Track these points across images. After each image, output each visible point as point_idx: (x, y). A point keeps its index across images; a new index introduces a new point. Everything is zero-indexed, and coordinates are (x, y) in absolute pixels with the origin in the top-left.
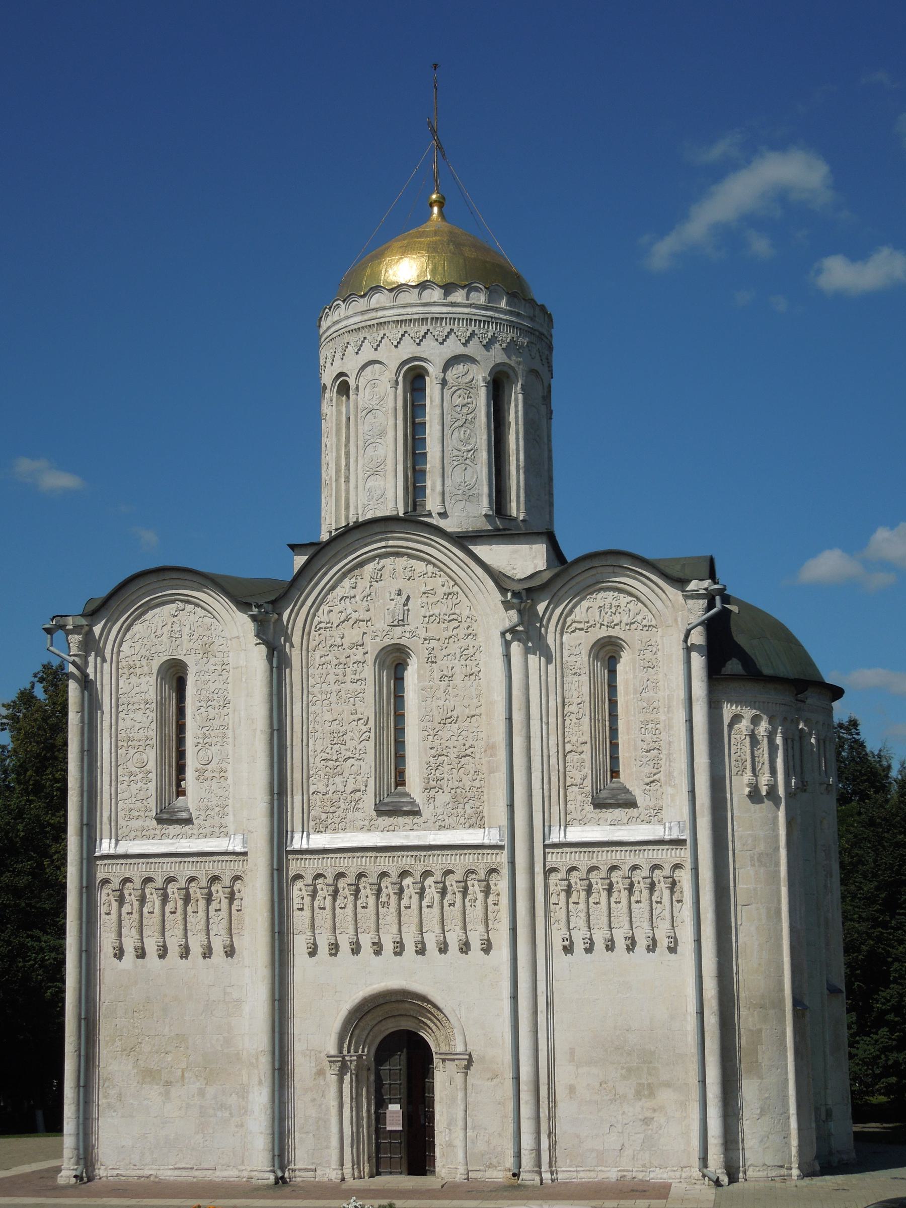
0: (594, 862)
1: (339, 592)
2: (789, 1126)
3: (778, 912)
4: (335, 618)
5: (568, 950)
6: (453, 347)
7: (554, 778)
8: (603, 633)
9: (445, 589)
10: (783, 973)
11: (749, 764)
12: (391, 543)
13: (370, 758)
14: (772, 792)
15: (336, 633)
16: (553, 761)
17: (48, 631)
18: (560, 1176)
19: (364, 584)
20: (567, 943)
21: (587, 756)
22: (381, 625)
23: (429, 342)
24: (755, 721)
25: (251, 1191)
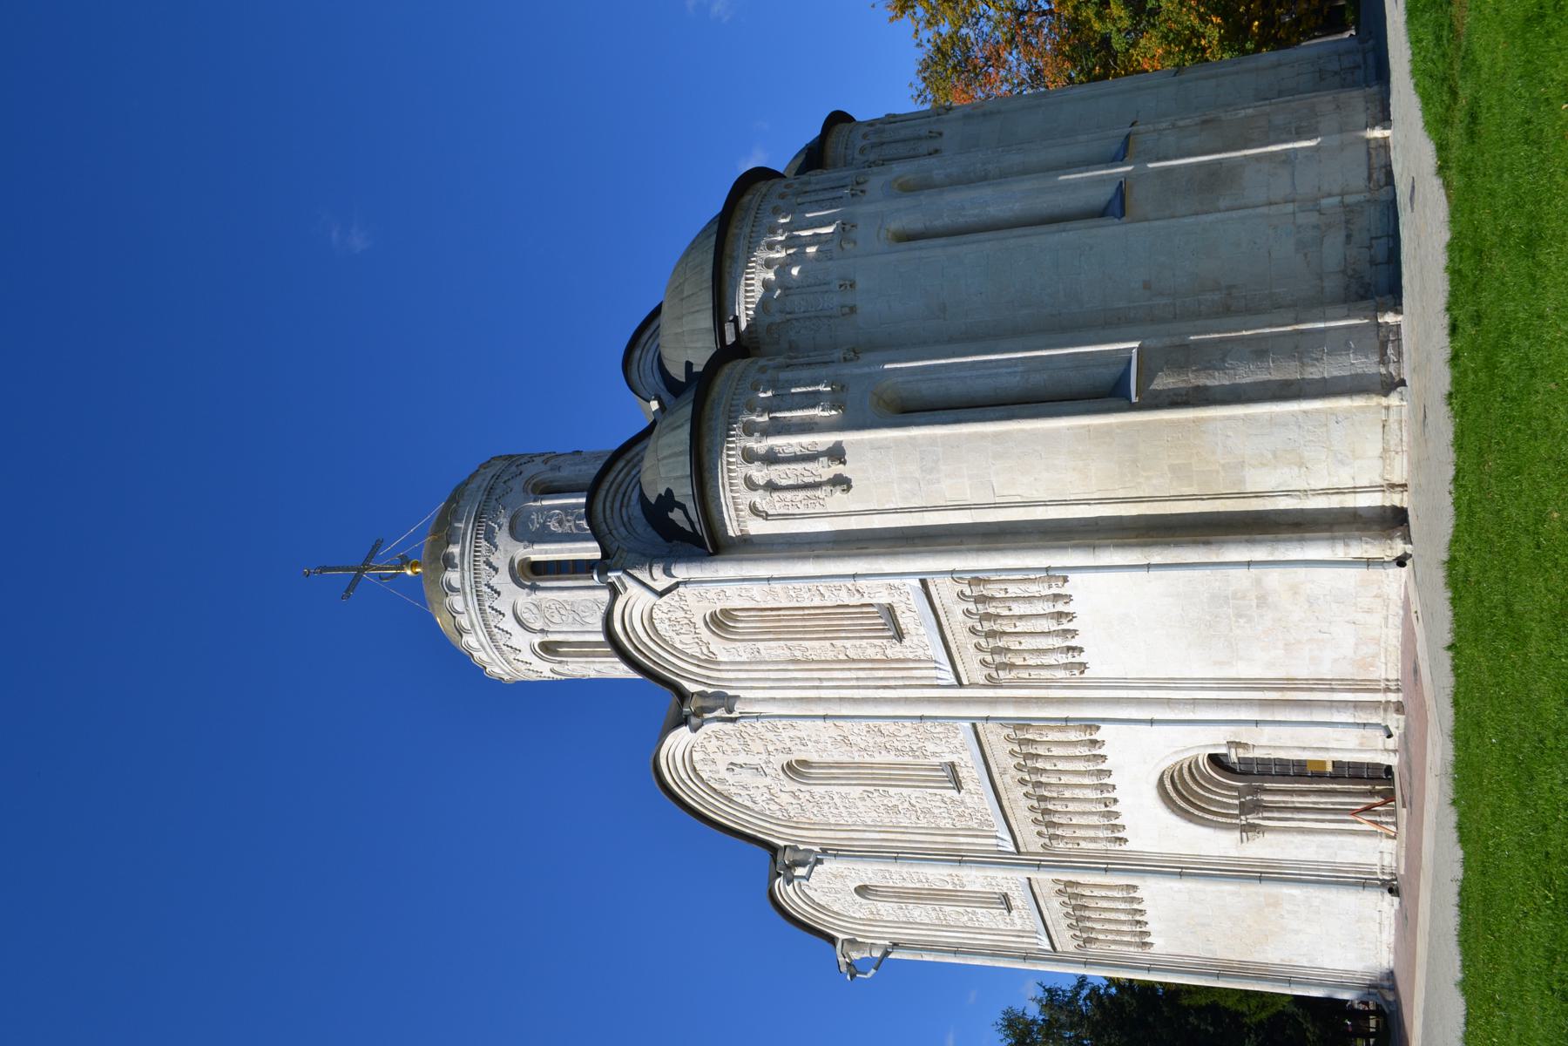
0: (971, 648)
1: (749, 804)
2: (1318, 411)
3: (996, 435)
4: (775, 807)
5: (1083, 667)
6: (509, 623)
7: (881, 674)
8: (705, 633)
9: (714, 740)
10: (1083, 427)
11: (810, 493)
12: (684, 776)
13: (905, 791)
14: (836, 454)
15: (790, 808)
16: (862, 674)
17: (853, 976)
18: (1393, 675)
19: (733, 790)
20: (1076, 672)
21: (848, 643)
22: (768, 781)
23: (514, 642)
24: (751, 484)
25: (1406, 922)
